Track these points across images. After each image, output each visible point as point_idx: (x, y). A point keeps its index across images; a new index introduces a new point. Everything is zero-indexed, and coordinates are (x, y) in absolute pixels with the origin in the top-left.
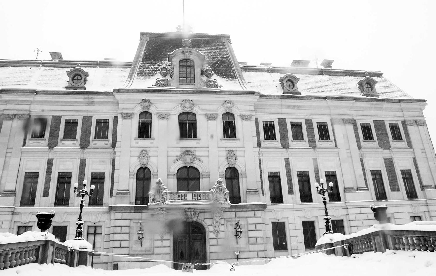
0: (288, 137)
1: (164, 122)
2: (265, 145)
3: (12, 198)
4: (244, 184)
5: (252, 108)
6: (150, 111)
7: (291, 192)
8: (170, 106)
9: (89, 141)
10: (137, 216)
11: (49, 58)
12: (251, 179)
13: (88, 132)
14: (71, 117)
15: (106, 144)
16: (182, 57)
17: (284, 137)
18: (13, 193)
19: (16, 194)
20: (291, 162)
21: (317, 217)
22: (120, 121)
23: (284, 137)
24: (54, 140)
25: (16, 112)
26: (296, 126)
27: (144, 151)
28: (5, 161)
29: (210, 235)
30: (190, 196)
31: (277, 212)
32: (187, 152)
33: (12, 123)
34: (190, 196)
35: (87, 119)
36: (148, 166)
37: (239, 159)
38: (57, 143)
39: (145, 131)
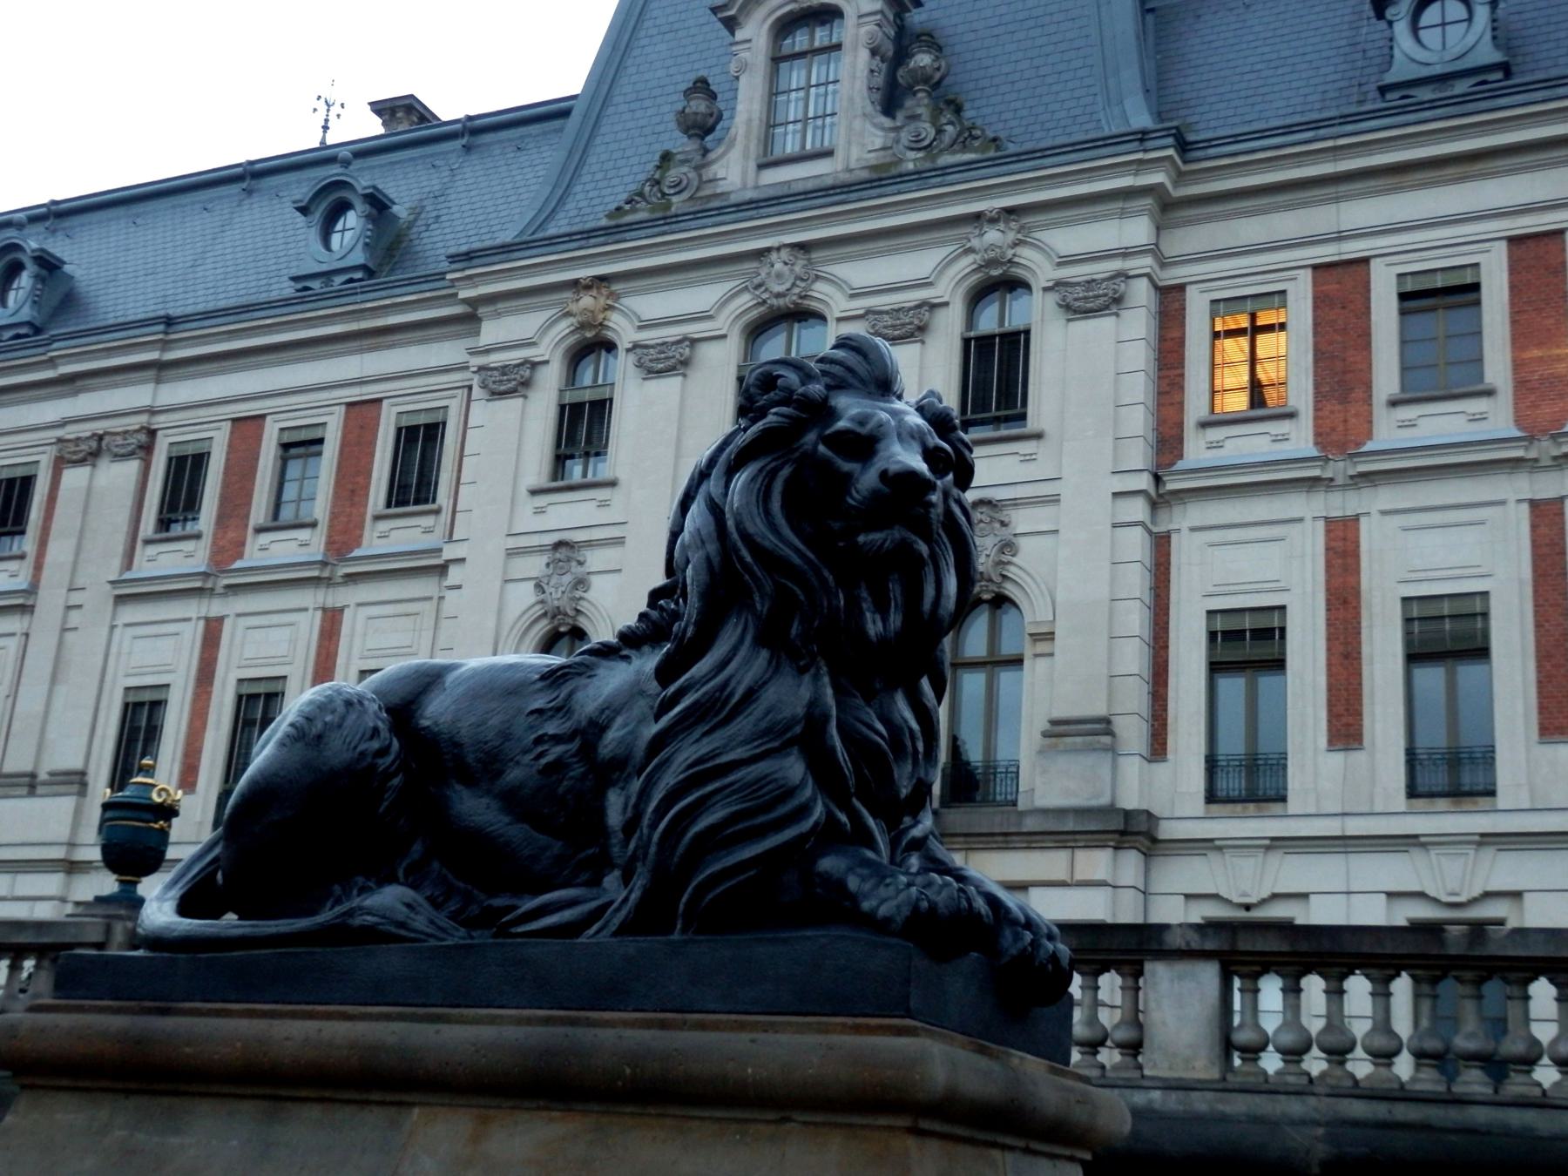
0: (1368, 385)
1: (672, 384)
2: (1211, 446)
3: (66, 804)
5: (1138, 230)
6: (610, 334)
7: (1346, 729)
9: (361, 526)
11: (373, 127)
13: (360, 479)
15: (428, 531)
18: (76, 781)
19: (84, 785)
20: (1371, 536)
21: (1517, 895)
24: (231, 535)
25: (99, 427)
26: (1441, 298)
28: (60, 644)
33: (92, 476)
35: (362, 413)
36: (583, 622)
37: (1023, 543)
38: (243, 544)
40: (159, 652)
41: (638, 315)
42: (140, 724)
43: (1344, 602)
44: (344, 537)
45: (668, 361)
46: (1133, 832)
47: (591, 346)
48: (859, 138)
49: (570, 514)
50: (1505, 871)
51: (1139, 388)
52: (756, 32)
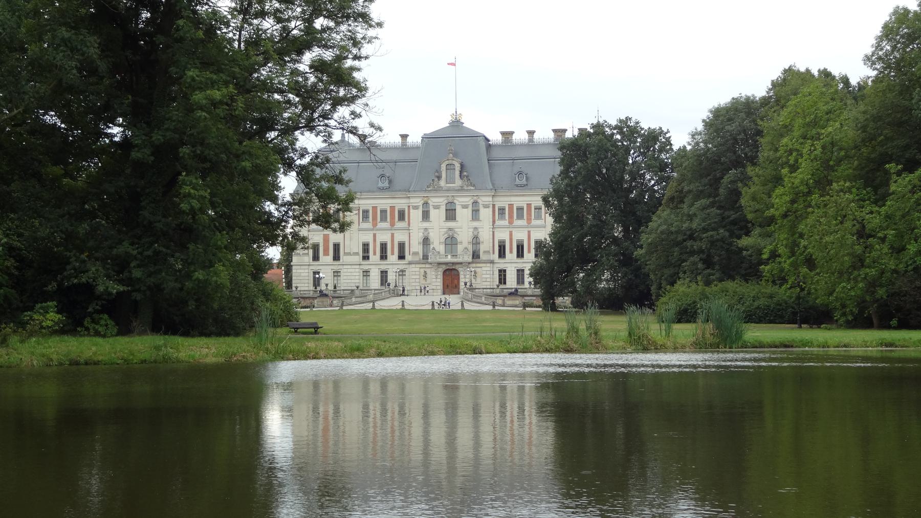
4: (483, 248)
5: (490, 199)
7: (511, 252)
8: (441, 200)
10: (423, 266)
12: (485, 246)
14: (383, 207)
16: (447, 162)
17: (511, 217)
18: (357, 254)
22: (412, 211)
23: (511, 217)
26: (520, 209)
27: (426, 229)
29: (461, 276)
30: (449, 257)
31: (501, 264)
32: (450, 229)
34: (449, 257)
35: (393, 208)
39: (426, 216)
40: (368, 238)
41: (433, 201)
42: (366, 247)
43: (511, 239)
44: (392, 224)
45: (437, 207)
46: (492, 262)
47: (426, 204)
48: (458, 182)
49: (426, 225)
50: (524, 265)
51: (491, 216)
52: (443, 166)
